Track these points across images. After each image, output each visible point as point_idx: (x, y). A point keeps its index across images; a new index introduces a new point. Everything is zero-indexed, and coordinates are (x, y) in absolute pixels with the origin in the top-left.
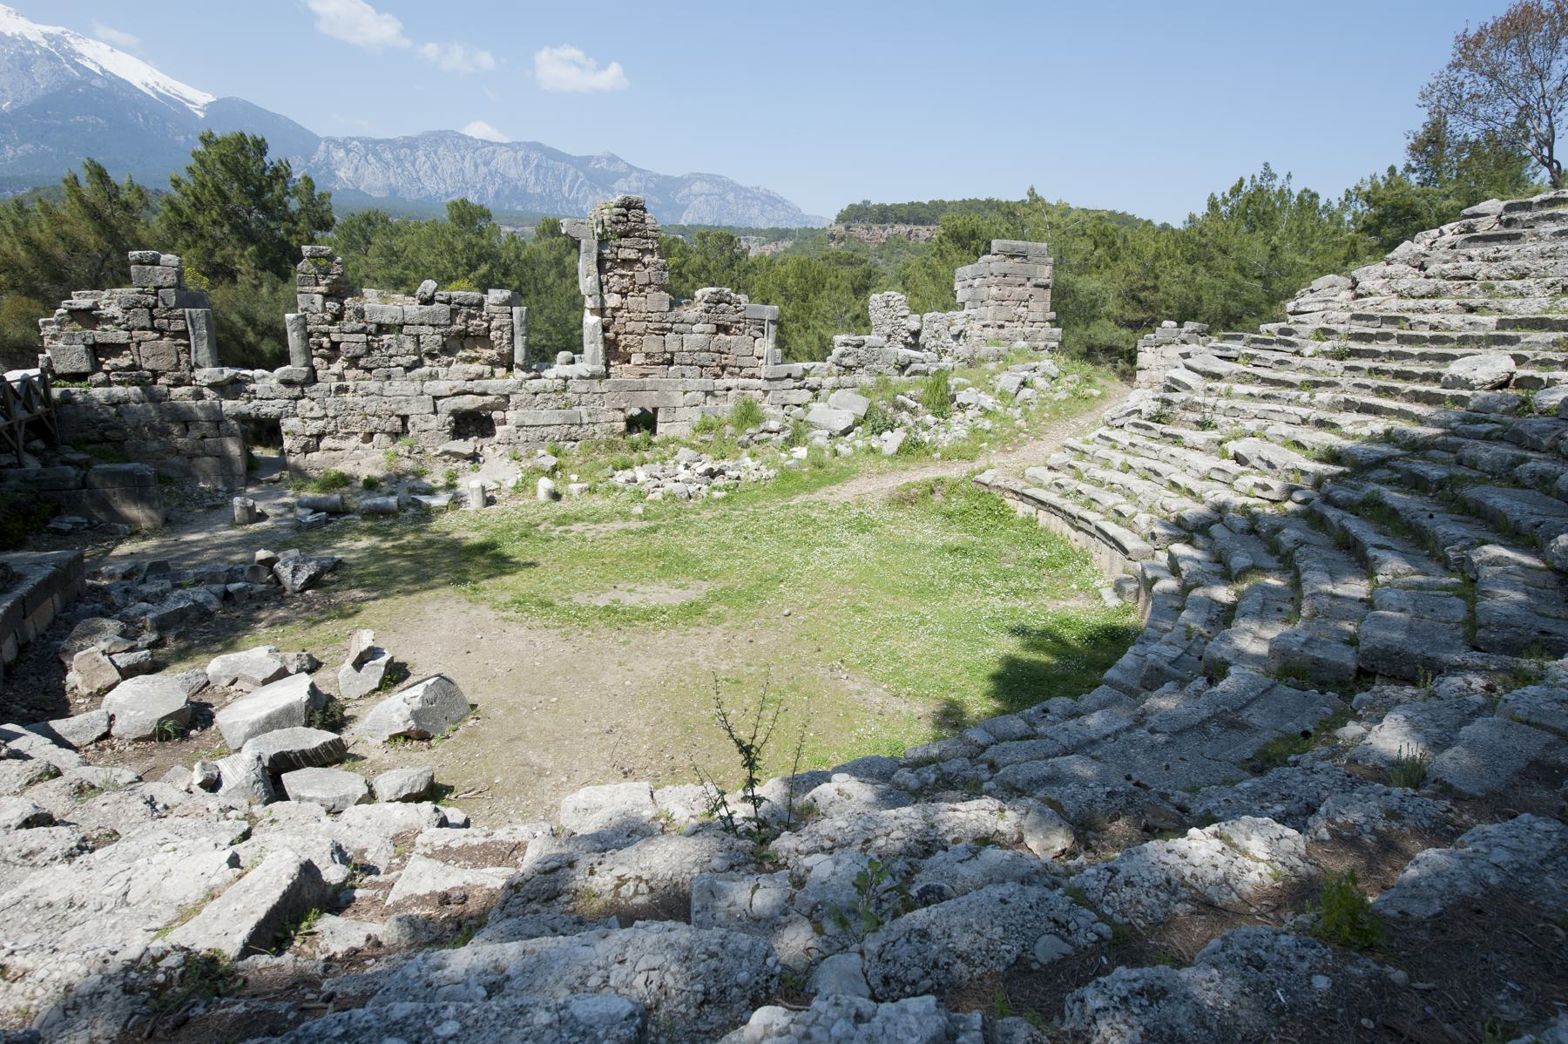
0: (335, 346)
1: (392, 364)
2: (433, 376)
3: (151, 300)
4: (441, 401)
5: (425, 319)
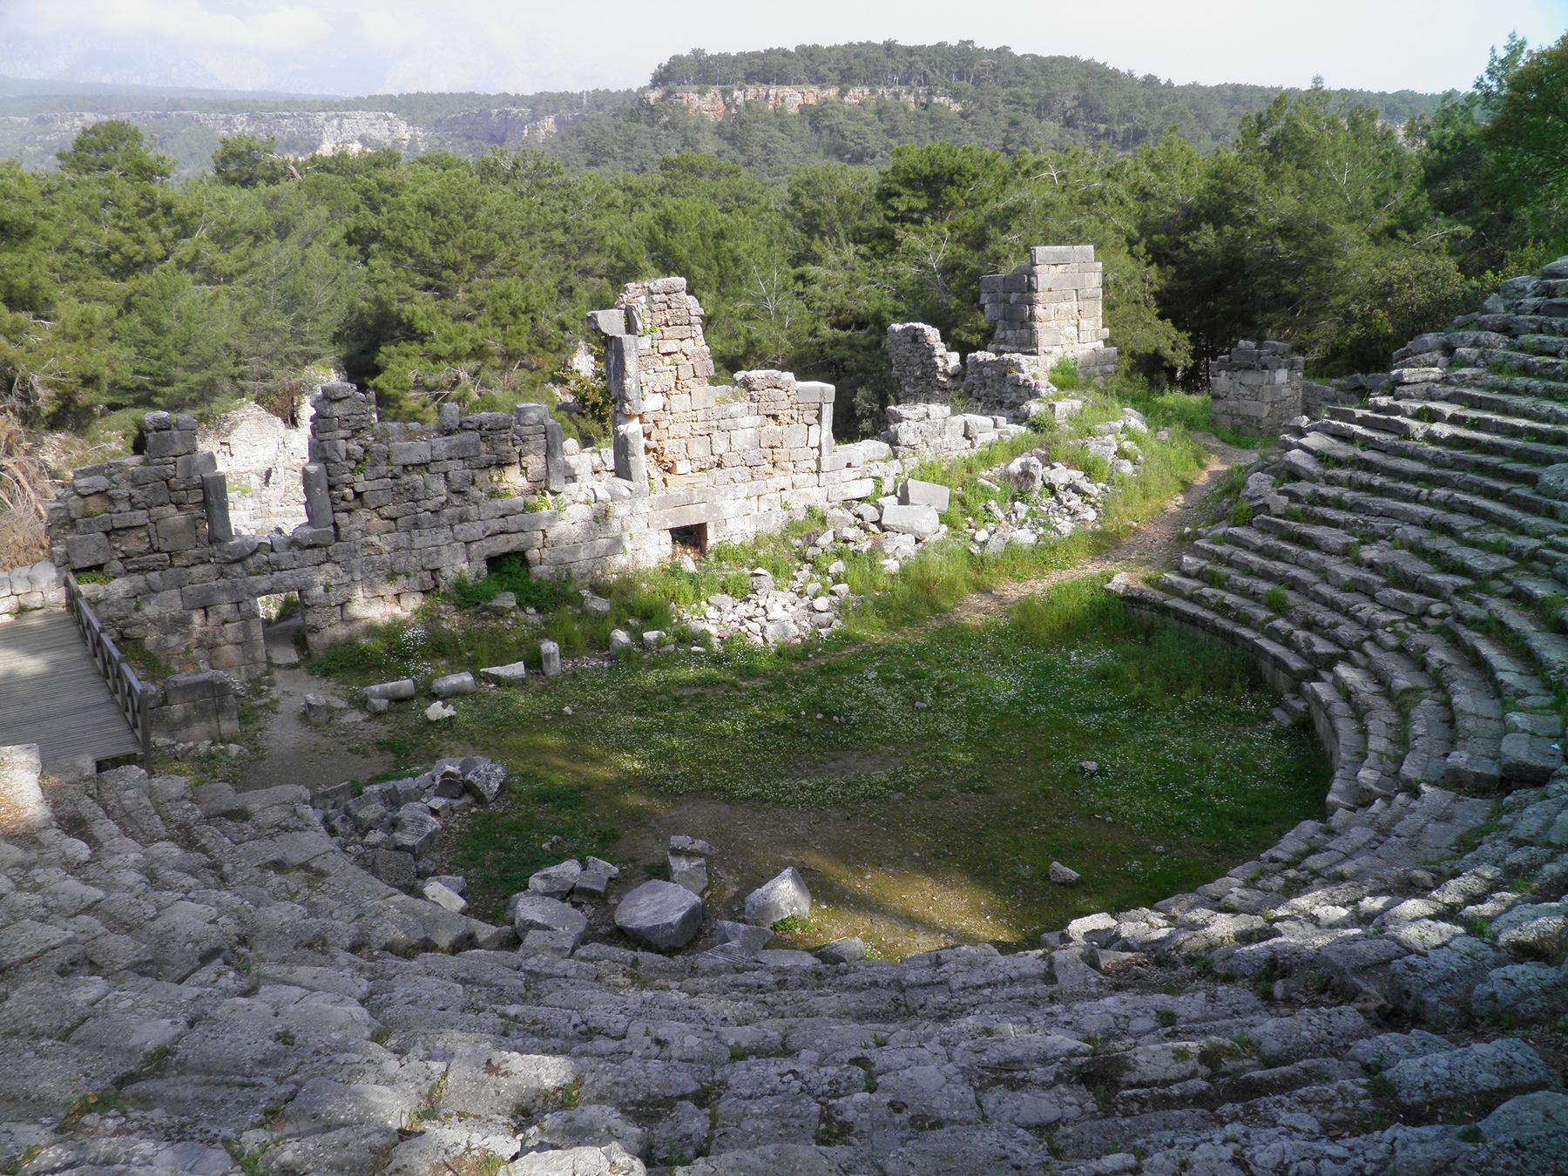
2: (463, 519)
4: (474, 546)
5: (453, 454)
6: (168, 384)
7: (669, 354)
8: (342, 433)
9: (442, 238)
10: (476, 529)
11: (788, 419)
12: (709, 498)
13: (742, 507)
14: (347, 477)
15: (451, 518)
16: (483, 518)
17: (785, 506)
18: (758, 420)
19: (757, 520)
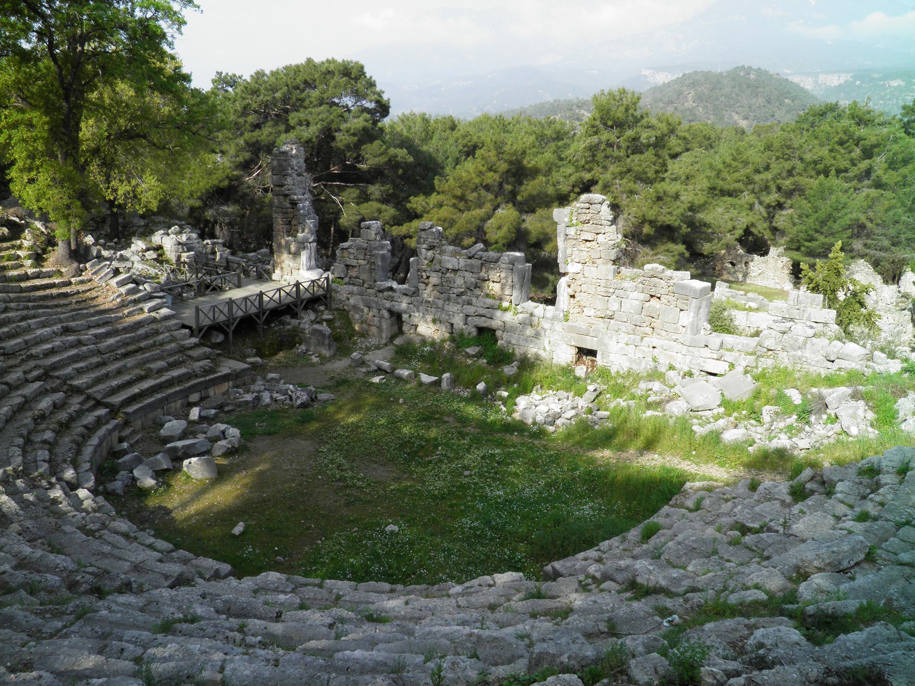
0: (428, 277)
2: (469, 303)
3: (365, 245)
4: (470, 318)
6: (810, 241)
7: (587, 241)
8: (425, 246)
10: (470, 310)
11: (666, 302)
12: (600, 336)
14: (424, 267)
15: (464, 301)
16: (479, 304)
17: (654, 360)
18: (642, 296)
19: (631, 360)
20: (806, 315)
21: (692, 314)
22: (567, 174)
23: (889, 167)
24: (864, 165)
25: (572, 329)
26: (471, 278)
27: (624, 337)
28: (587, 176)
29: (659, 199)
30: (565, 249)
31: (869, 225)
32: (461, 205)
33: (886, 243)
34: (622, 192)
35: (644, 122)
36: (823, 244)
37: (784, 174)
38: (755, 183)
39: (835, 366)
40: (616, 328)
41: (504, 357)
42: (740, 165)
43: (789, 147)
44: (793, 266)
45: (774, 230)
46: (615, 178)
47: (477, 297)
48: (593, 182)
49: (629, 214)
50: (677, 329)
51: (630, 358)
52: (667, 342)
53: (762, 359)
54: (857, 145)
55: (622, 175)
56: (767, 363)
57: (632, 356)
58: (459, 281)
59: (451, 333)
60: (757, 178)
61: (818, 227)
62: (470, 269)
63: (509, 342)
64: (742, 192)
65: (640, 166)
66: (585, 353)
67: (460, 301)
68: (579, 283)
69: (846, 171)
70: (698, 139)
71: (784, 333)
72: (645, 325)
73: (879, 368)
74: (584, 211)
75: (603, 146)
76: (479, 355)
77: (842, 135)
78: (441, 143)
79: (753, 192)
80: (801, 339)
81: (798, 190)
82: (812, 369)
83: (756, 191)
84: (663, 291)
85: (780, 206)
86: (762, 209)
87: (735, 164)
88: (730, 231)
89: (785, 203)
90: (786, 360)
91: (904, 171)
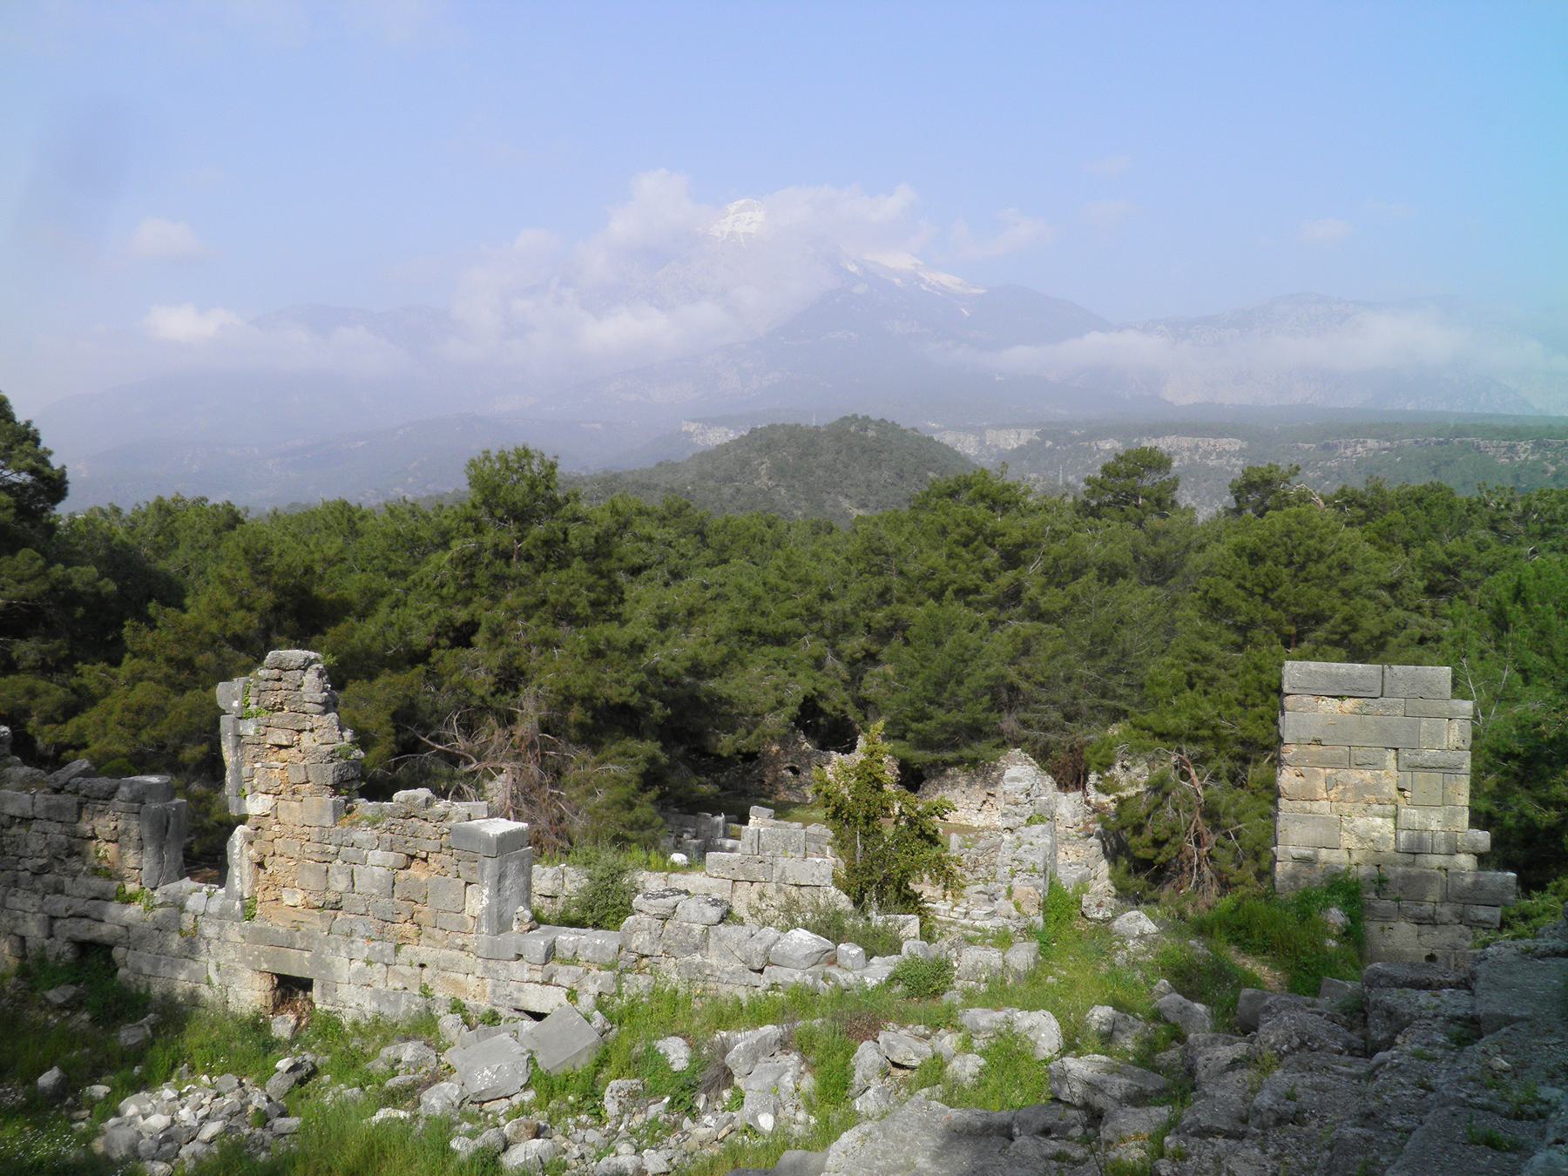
1: (20, 867)
2: (58, 890)
4: (58, 923)
7: (281, 747)
9: (1257, 590)
10: (59, 904)
12: (316, 946)
13: (359, 973)
15: (46, 886)
17: (425, 992)
18: (391, 858)
19: (379, 997)
20: (776, 873)
21: (486, 891)
22: (424, 611)
23: (1049, 582)
24: (1006, 579)
25: (259, 937)
26: (57, 833)
27: (362, 947)
28: (461, 615)
29: (597, 654)
30: (239, 766)
31: (1024, 685)
32: (184, 676)
33: (1056, 716)
34: (528, 646)
35: (566, 511)
36: (944, 724)
37: (873, 601)
38: (823, 619)
39: (764, 981)
40: (346, 929)
41: (129, 1005)
42: (794, 587)
43: (877, 552)
44: (899, 767)
45: (863, 704)
46: (514, 617)
47: (74, 875)
48: (472, 626)
49: (540, 686)
50: (463, 923)
51: (378, 991)
52: (448, 952)
53: (629, 977)
54: (992, 546)
55: (528, 611)
56: (638, 983)
57: (381, 987)
58: (36, 843)
59: (24, 957)
60: (827, 608)
61: (931, 694)
62: (55, 813)
63: (139, 972)
64: (800, 636)
65: (560, 592)
66: (290, 987)
67: (38, 885)
68: (269, 835)
69: (977, 590)
70: (743, 542)
71: (665, 919)
72: (402, 918)
73: (845, 978)
74: (270, 684)
75: (487, 557)
76: (74, 1005)
77: (964, 529)
78: (193, 555)
79: (820, 634)
80: (698, 928)
81: (898, 627)
82: (724, 990)
83: (827, 632)
84: (431, 845)
85: (871, 658)
86: (840, 666)
87: (784, 585)
88: (773, 709)
89: (878, 652)
90: (674, 976)
91: (1076, 587)
